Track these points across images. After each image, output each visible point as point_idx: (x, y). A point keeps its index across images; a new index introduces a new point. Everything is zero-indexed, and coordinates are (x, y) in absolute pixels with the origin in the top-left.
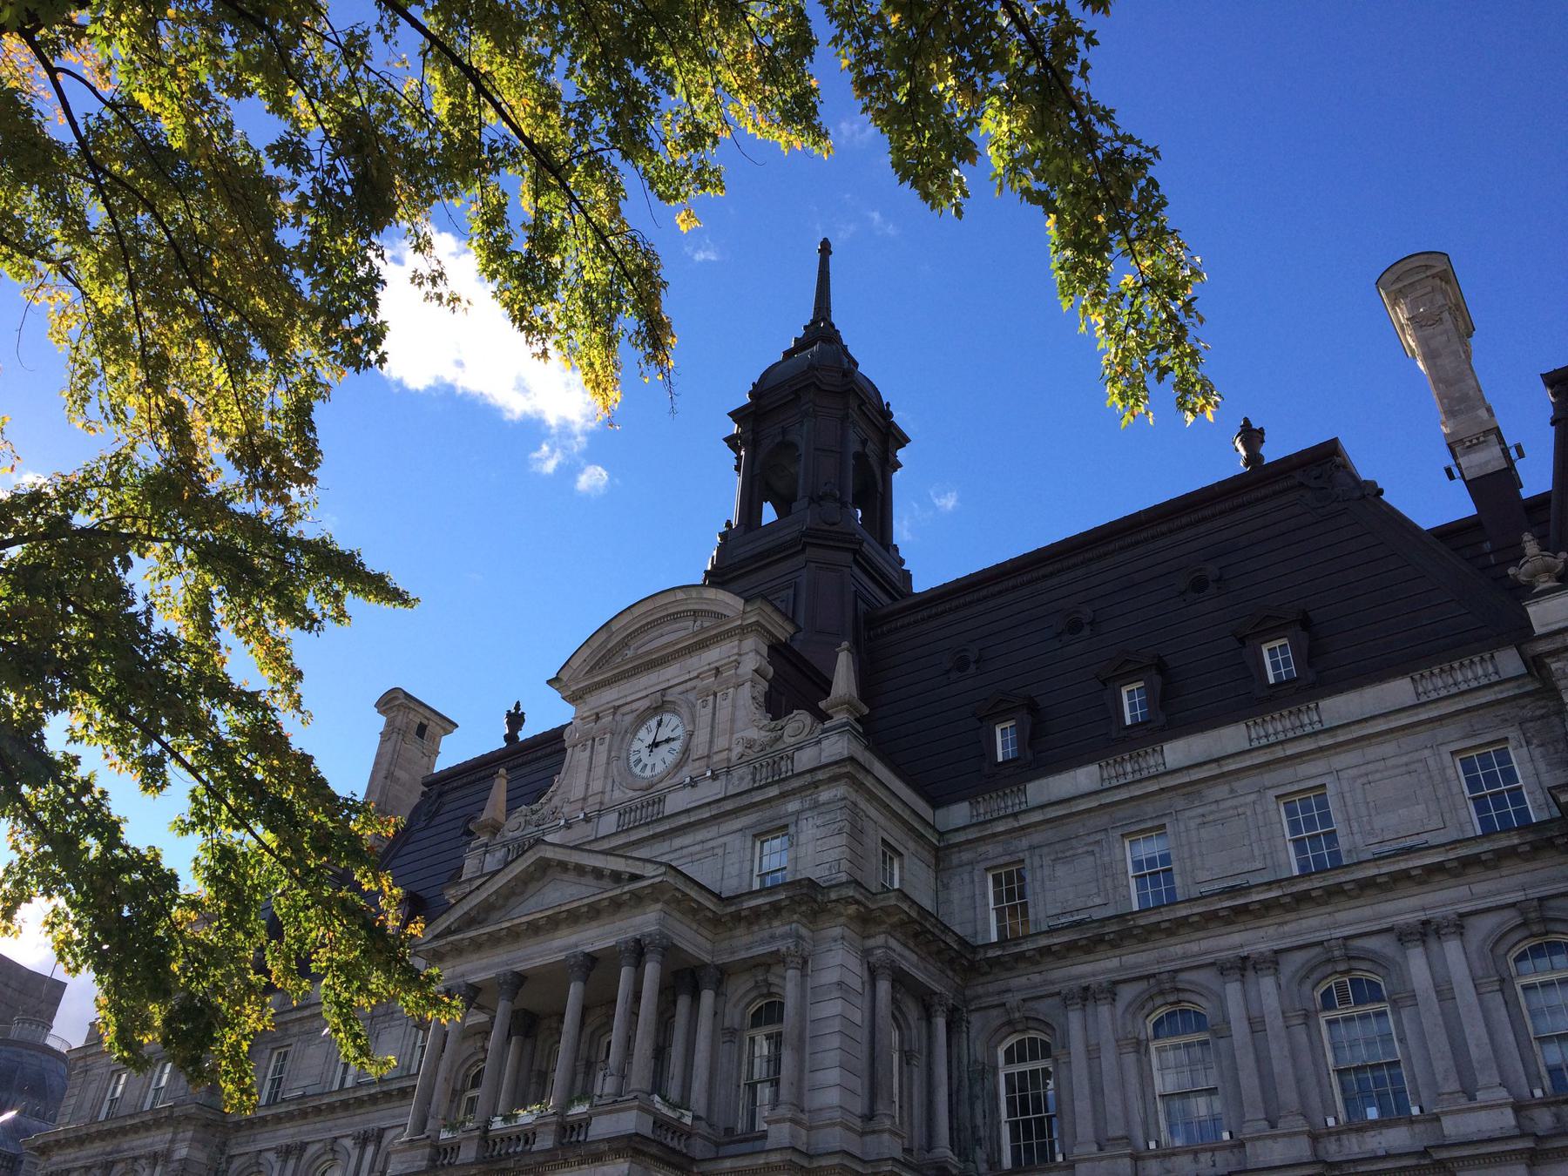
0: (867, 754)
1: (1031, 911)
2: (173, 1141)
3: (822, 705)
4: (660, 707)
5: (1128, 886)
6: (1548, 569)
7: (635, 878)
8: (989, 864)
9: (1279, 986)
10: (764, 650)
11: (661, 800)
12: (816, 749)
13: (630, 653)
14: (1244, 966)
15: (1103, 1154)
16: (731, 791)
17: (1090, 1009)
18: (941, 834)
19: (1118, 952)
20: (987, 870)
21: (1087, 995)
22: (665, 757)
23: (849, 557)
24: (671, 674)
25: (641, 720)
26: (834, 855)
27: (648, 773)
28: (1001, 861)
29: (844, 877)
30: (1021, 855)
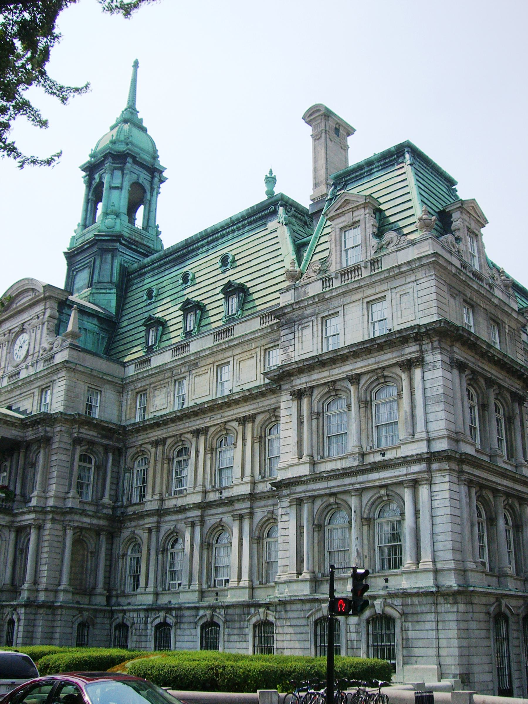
4: (22, 331)
9: (206, 440)
10: (56, 306)
14: (197, 433)
18: (122, 380)
19: (167, 427)
22: (23, 352)
24: (25, 316)
25: (18, 335)
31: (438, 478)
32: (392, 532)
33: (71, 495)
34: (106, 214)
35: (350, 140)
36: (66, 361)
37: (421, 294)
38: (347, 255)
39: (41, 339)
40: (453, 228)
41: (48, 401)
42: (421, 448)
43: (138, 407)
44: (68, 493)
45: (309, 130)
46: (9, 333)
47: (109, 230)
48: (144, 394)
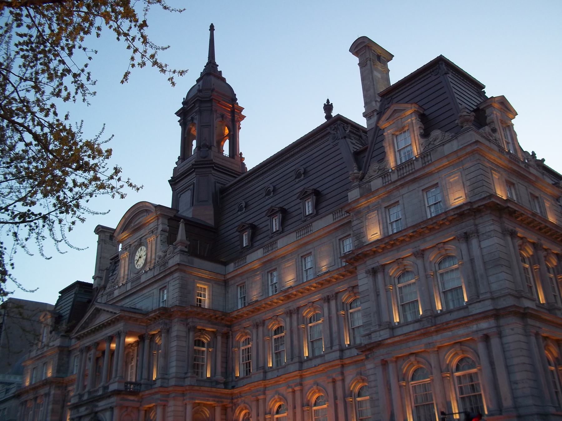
0: (190, 258)
2: (50, 389)
4: (140, 245)
5: (268, 289)
6: (357, 178)
7: (115, 313)
8: (237, 284)
10: (166, 221)
13: (133, 225)
20: (238, 286)
27: (139, 268)
28: (241, 282)
31: (507, 331)
32: (471, 383)
33: (189, 374)
34: (198, 147)
35: (390, 64)
36: (178, 264)
37: (468, 177)
38: (400, 155)
39: (156, 249)
40: (488, 121)
41: (165, 298)
42: (488, 306)
43: (239, 297)
44: (186, 373)
45: (356, 60)
46: (130, 247)
47: (203, 160)
48: (243, 286)
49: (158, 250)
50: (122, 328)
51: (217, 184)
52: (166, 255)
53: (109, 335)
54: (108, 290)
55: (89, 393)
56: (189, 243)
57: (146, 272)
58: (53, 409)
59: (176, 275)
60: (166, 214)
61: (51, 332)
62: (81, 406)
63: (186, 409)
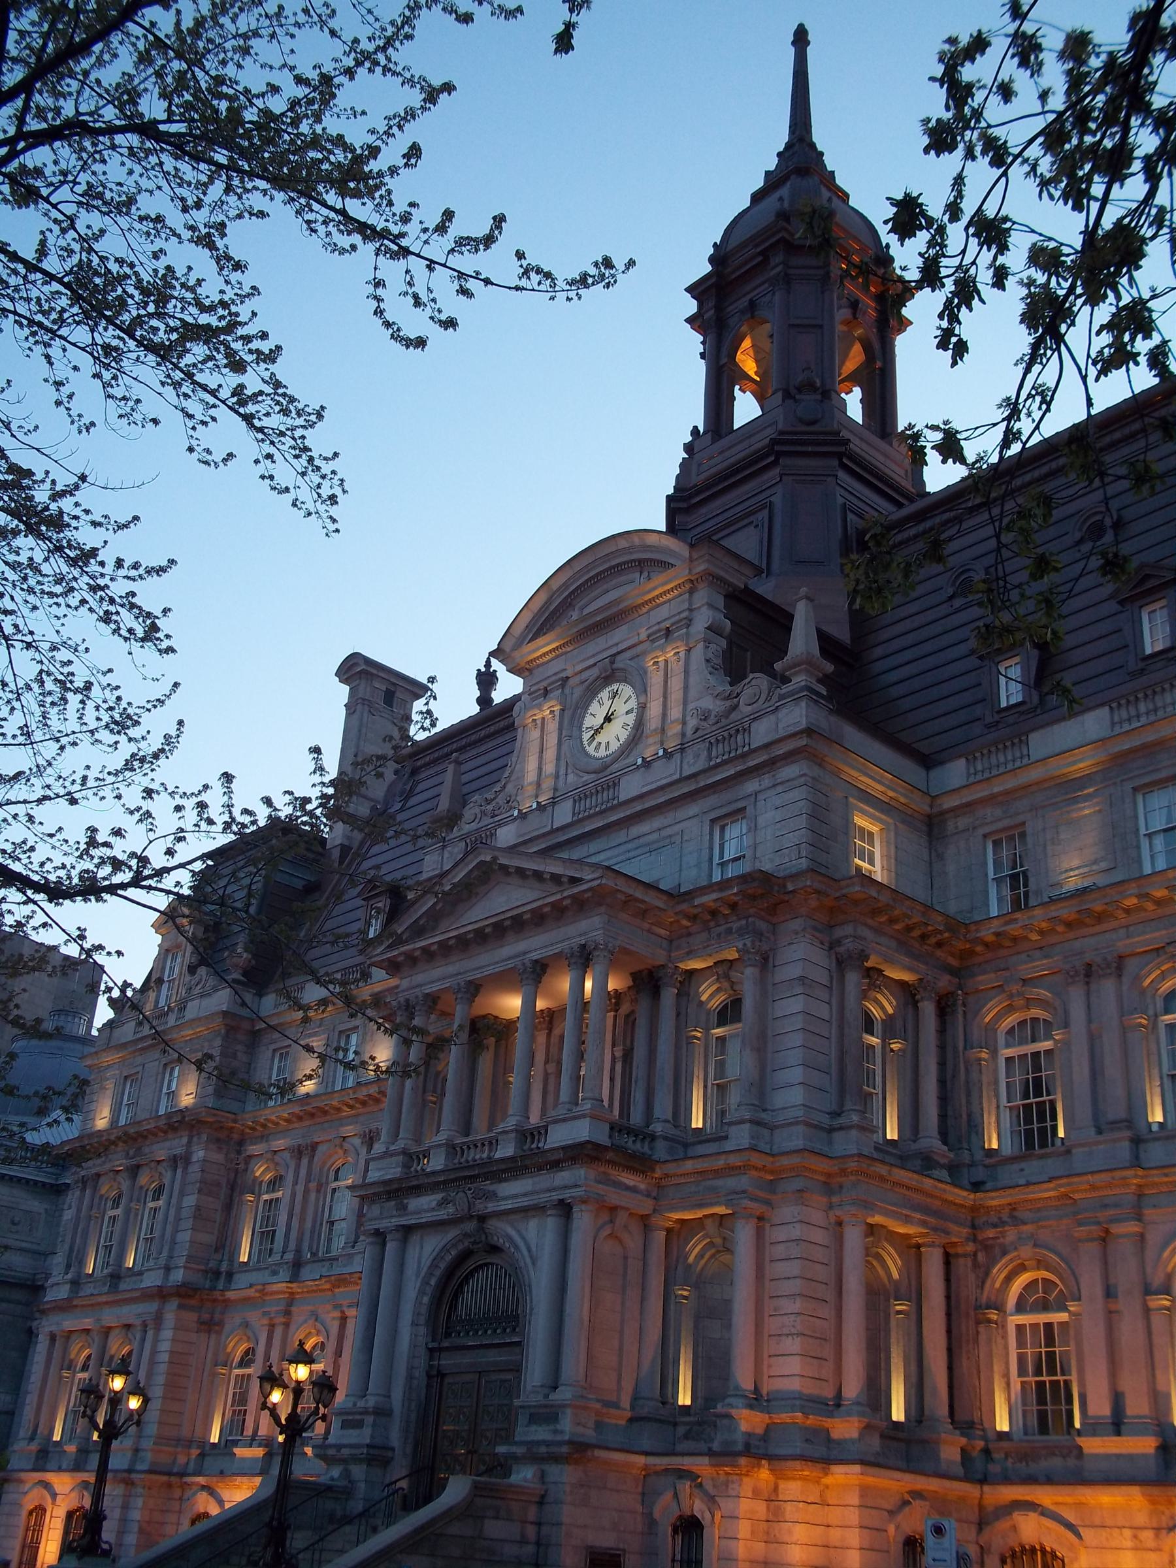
0: (833, 719)
1: (1032, 880)
3: (778, 666)
4: (610, 675)
5: (1138, 847)
7: (574, 881)
8: (987, 830)
10: (720, 602)
11: (615, 784)
12: (772, 718)
15: (1100, 1138)
16: (687, 771)
17: (1093, 986)
20: (985, 836)
21: (1089, 973)
23: (836, 463)
25: (591, 692)
26: (794, 838)
27: (602, 753)
28: (1000, 825)
29: (804, 863)
30: (1021, 818)
39: (686, 688)
43: (991, 875)
46: (563, 686)
49: (693, 693)
50: (598, 935)
51: (850, 516)
52: (735, 708)
53: (535, 956)
54: (465, 827)
55: (452, 1148)
56: (829, 668)
57: (647, 764)
58: (198, 1208)
59: (790, 771)
60: (722, 573)
61: (192, 970)
62: (417, 1190)
63: (839, 1240)
